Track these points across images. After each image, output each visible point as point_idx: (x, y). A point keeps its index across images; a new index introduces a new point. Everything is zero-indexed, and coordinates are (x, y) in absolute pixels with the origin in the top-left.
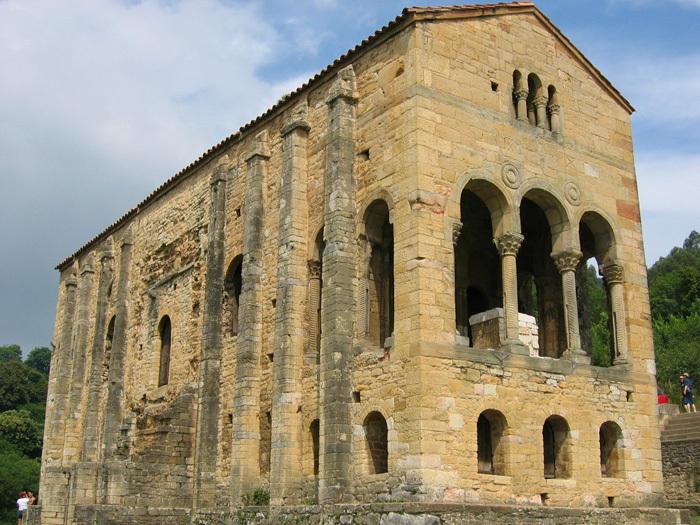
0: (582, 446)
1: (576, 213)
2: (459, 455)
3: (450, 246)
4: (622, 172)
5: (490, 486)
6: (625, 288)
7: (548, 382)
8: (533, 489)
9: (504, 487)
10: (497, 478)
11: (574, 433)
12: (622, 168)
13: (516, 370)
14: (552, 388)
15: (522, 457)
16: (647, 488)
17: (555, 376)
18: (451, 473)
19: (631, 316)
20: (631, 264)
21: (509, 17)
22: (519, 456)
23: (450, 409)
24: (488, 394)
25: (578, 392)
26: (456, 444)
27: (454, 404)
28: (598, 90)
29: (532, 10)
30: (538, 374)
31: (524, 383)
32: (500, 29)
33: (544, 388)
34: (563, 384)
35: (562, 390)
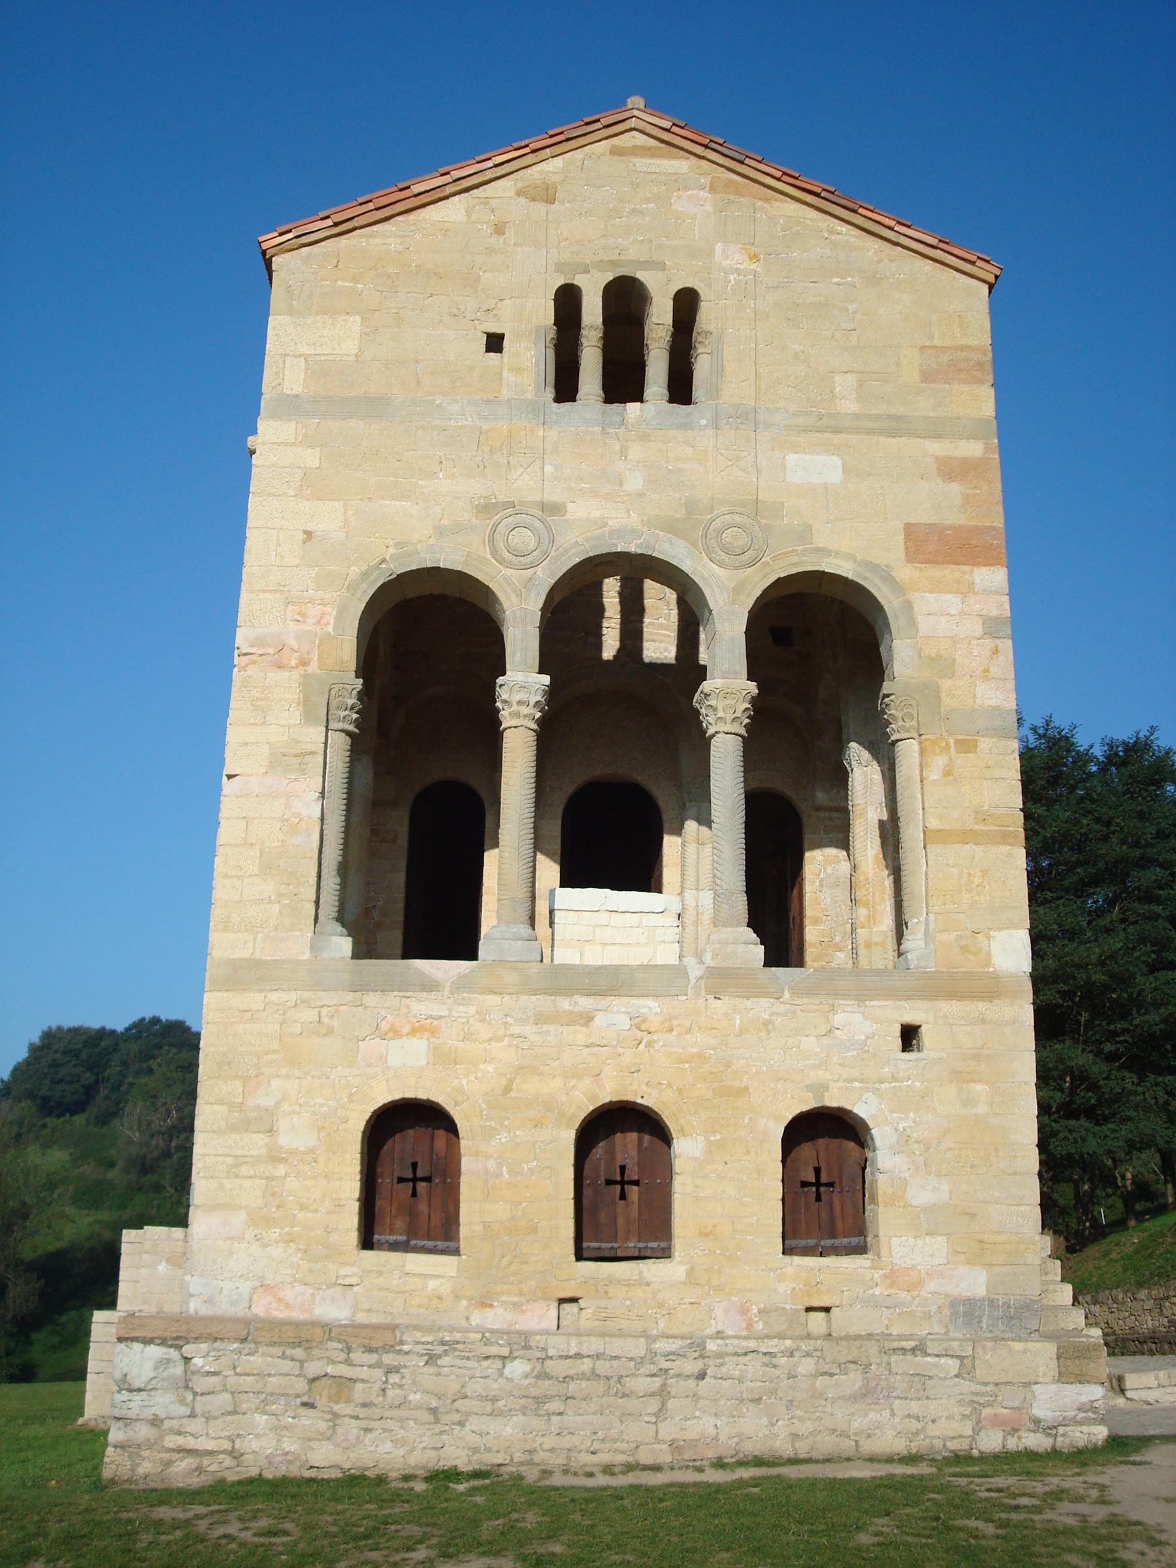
0: (726, 1182)
1: (738, 590)
2: (303, 1207)
3: (316, 734)
4: (936, 448)
7: (600, 1020)
9: (432, 1284)
10: (417, 1262)
13: (492, 1000)
15: (500, 1211)
16: (974, 1282)
18: (277, 1251)
19: (934, 823)
20: (946, 684)
21: (558, 162)
23: (286, 1107)
26: (292, 1183)
29: (633, 123)
30: (565, 1004)
31: (517, 1030)
33: (579, 1035)
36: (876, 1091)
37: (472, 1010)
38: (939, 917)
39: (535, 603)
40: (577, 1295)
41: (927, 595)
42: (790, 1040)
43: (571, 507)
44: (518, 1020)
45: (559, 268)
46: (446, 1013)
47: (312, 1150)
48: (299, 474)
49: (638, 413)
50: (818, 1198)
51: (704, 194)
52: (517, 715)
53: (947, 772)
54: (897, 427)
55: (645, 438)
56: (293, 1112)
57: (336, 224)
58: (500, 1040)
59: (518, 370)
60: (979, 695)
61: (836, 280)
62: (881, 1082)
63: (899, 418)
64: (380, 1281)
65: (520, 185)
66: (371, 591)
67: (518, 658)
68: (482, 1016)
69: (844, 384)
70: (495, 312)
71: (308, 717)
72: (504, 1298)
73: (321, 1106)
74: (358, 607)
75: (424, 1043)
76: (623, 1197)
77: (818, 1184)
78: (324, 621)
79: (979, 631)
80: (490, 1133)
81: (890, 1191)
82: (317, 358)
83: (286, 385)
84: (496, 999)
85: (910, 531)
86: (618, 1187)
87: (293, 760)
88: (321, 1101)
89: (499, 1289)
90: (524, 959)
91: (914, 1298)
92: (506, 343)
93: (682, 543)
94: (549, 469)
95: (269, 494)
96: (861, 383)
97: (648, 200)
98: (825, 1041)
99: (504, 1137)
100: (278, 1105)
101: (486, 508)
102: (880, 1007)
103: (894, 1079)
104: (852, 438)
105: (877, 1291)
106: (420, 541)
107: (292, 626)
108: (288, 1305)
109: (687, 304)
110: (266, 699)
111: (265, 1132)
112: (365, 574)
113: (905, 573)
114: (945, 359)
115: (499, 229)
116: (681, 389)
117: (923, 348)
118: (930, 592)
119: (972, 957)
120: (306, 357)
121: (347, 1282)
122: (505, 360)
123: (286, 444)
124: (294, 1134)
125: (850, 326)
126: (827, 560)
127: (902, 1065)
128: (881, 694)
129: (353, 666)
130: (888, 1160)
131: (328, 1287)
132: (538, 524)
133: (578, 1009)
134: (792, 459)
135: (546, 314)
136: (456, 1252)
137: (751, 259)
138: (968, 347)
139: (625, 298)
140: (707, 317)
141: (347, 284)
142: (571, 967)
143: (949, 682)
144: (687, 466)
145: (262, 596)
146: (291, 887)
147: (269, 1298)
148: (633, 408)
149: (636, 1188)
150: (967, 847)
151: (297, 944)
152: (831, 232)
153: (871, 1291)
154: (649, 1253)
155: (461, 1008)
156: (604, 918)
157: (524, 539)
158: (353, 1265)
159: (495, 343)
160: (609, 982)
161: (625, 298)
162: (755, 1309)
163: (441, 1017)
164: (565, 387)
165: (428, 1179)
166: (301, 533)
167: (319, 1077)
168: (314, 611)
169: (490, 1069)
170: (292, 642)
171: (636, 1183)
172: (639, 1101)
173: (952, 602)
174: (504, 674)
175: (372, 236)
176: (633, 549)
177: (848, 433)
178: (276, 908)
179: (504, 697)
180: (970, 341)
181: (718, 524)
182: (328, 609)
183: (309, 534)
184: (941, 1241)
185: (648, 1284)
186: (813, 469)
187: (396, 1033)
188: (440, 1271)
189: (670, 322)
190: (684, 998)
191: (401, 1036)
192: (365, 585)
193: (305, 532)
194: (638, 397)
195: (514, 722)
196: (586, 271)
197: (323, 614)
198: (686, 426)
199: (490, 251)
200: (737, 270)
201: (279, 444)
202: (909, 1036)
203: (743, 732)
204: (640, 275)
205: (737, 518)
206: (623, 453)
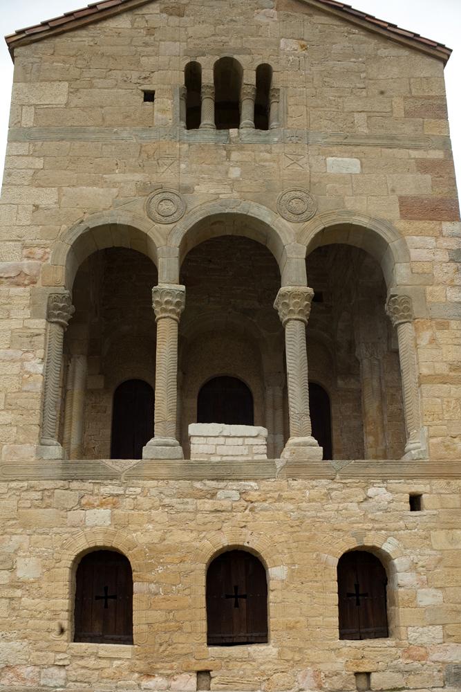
0: (302, 596)
1: (299, 235)
2: (32, 617)
3: (40, 324)
4: (415, 154)
5: (91, 662)
6: (416, 329)
7: (220, 494)
8: (175, 664)
9: (116, 663)
11: (276, 573)
12: (416, 148)
14: (227, 503)
15: (157, 615)
17: (235, 485)
18: (16, 645)
19: (425, 371)
20: (429, 289)
22: (150, 613)
23: (21, 553)
24: (96, 526)
25: (292, 507)
26: (26, 601)
27: (26, 545)
28: (372, 44)
30: (198, 485)
31: (167, 501)
32: (165, 15)
33: (208, 504)
34: (254, 495)
35: (251, 505)
36: (394, 536)
37: (139, 490)
38: (430, 428)
39: (176, 241)
40: (210, 669)
41: (414, 237)
42: (341, 505)
43: (196, 188)
44: (167, 496)
45: (186, 54)
46: (122, 492)
47: (38, 580)
48: (31, 172)
49: (236, 135)
50: (358, 604)
51: (273, 11)
52: (164, 310)
53: (433, 340)
54: (391, 142)
55: (241, 149)
56: (25, 557)
57: (52, 29)
58: (157, 509)
59: (163, 111)
60: (449, 295)
61: (353, 60)
62: (401, 529)
63: (393, 138)
64: (82, 663)
65: (163, 6)
66: (74, 238)
67: (165, 276)
68: (145, 492)
69: (360, 118)
70: (149, 79)
71: (35, 315)
72: (161, 672)
73: (44, 552)
74: (66, 248)
75: (109, 511)
76: (237, 605)
77: (357, 595)
78: (45, 257)
79: (447, 258)
80: (151, 568)
81: (406, 598)
82: (42, 106)
83: (23, 122)
84: (154, 483)
85: (403, 201)
86: (234, 599)
87: (25, 340)
88: (44, 549)
89: (158, 666)
90: (171, 457)
91: (423, 665)
92: (155, 96)
93: (264, 207)
94: (183, 166)
95: (12, 185)
96: (369, 117)
97: (241, 14)
98: (364, 505)
99: (160, 570)
100: (16, 552)
101: (144, 189)
102: (396, 483)
103: (407, 528)
104: (366, 149)
105: (401, 660)
106: (104, 209)
107: (26, 261)
108: (24, 679)
109: (264, 73)
110: (9, 303)
111: (8, 569)
112: (71, 229)
113: (401, 225)
114: (419, 103)
115: (150, 31)
116: (262, 120)
117: (405, 98)
118: (417, 236)
119: (451, 452)
120: (35, 105)
121: (61, 663)
122: (155, 105)
123: (24, 155)
124: (27, 569)
125: (362, 86)
126: (353, 218)
127: (412, 519)
128: (389, 296)
129: (63, 283)
130: (403, 578)
131: (49, 667)
132: (176, 198)
133: (205, 488)
134: (330, 159)
135: (180, 79)
136: (130, 641)
137: (302, 48)
138: (433, 97)
139: (227, 70)
140: (277, 80)
141: (60, 64)
142: (201, 463)
143: (431, 288)
144: (267, 164)
145: (7, 243)
146: (24, 416)
147: (11, 675)
148: (233, 132)
149: (244, 600)
150: (445, 385)
151: (28, 451)
152: (349, 33)
153: (395, 662)
154: (253, 640)
155: (131, 489)
156: (221, 440)
157: (167, 207)
158: (65, 652)
159: (149, 96)
160: (224, 472)
161: (227, 70)
162: (322, 675)
163: (118, 495)
164: (193, 121)
165: (114, 597)
166: (31, 206)
167: (41, 534)
168: (39, 252)
169: (150, 526)
170: (26, 271)
171: (245, 597)
172: (246, 544)
173: (431, 241)
174: (157, 285)
175: (74, 37)
176: (235, 211)
177: (363, 146)
178: (15, 429)
179: (158, 299)
180: (433, 94)
181: (287, 197)
182: (48, 250)
183: (37, 207)
184: (439, 628)
185: (254, 660)
186: (344, 164)
187: (91, 506)
188: (121, 655)
189: (255, 83)
190: (273, 480)
191: (94, 507)
192: (71, 236)
193: (34, 205)
194: (236, 124)
195: (163, 315)
196: (203, 55)
197: (45, 253)
198: (266, 142)
199: (146, 44)
200: (293, 54)
201: (18, 156)
202: (415, 502)
203: (305, 319)
204: (235, 57)
205: (298, 194)
206: (228, 156)
